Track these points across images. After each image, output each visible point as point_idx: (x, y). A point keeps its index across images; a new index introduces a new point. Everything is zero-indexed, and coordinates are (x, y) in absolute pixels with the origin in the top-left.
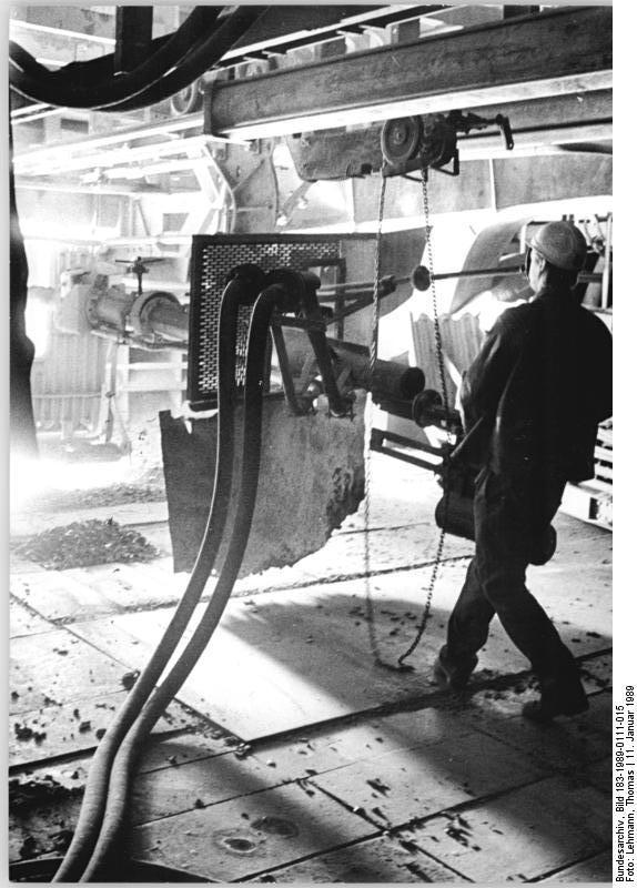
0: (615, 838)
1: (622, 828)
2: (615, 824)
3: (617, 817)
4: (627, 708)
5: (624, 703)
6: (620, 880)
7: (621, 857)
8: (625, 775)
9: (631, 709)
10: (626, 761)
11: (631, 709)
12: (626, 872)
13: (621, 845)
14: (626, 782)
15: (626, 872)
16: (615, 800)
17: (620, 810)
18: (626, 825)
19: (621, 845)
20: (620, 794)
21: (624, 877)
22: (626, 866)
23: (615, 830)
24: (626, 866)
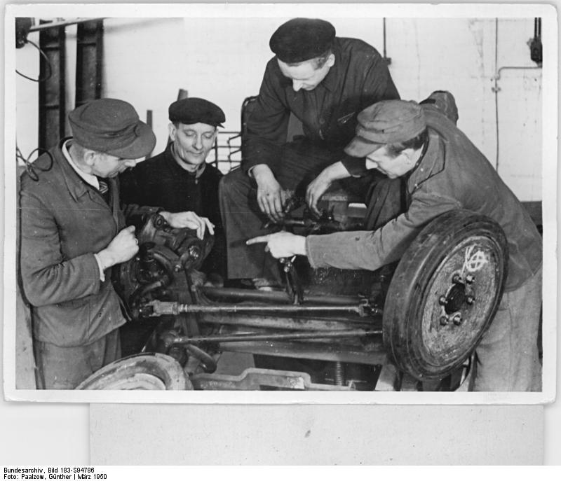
1: (38, 471)
4: (90, 474)
5: (96, 473)
6: (5, 470)
7: (20, 471)
8: (69, 474)
9: (92, 477)
10: (77, 474)
11: (92, 477)
12: (10, 474)
13: (27, 471)
14: (66, 474)
15: (10, 474)
17: (50, 470)
18: (40, 474)
19: (27, 471)
20: (59, 470)
21: (7, 473)
22: (13, 474)
24: (13, 474)
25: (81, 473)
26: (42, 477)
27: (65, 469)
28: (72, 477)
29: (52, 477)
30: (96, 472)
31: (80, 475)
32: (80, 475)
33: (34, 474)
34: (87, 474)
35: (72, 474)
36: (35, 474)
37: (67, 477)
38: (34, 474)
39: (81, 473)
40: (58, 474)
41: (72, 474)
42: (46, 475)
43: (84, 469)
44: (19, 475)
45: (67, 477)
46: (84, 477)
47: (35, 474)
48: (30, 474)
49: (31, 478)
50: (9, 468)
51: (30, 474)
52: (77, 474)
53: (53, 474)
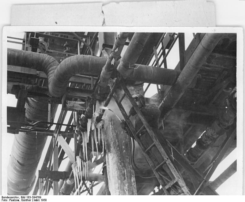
0: (14, 196)
1: (16, 198)
2: (18, 196)
3: (20, 196)
5: (42, 198)
6: (2, 197)
7: (9, 197)
8: (30, 199)
9: (40, 200)
10: (33, 199)
11: (40, 200)
12: (4, 199)
13: (12, 198)
14: (29, 199)
15: (4, 199)
16: (24, 196)
17: (22, 197)
18: (17, 199)
19: (12, 198)
20: (26, 197)
21: (3, 198)
22: (6, 199)
23: (16, 196)
24: (6, 199)
25: (35, 199)
26: (18, 200)
27: (29, 197)
28: (32, 200)
29: (23, 200)
30: (42, 198)
31: (35, 200)
32: (35, 200)
33: (15, 199)
34: (38, 199)
35: (31, 199)
36: (15, 199)
37: (29, 200)
38: (15, 199)
39: (35, 199)
40: (25, 199)
41: (31, 199)
42: (20, 199)
43: (37, 197)
44: (8, 199)
45: (29, 200)
46: (37, 200)
47: (15, 199)
48: (13, 199)
49: (13, 200)
50: (4, 196)
51: (13, 199)
52: (33, 199)
53: (23, 199)
